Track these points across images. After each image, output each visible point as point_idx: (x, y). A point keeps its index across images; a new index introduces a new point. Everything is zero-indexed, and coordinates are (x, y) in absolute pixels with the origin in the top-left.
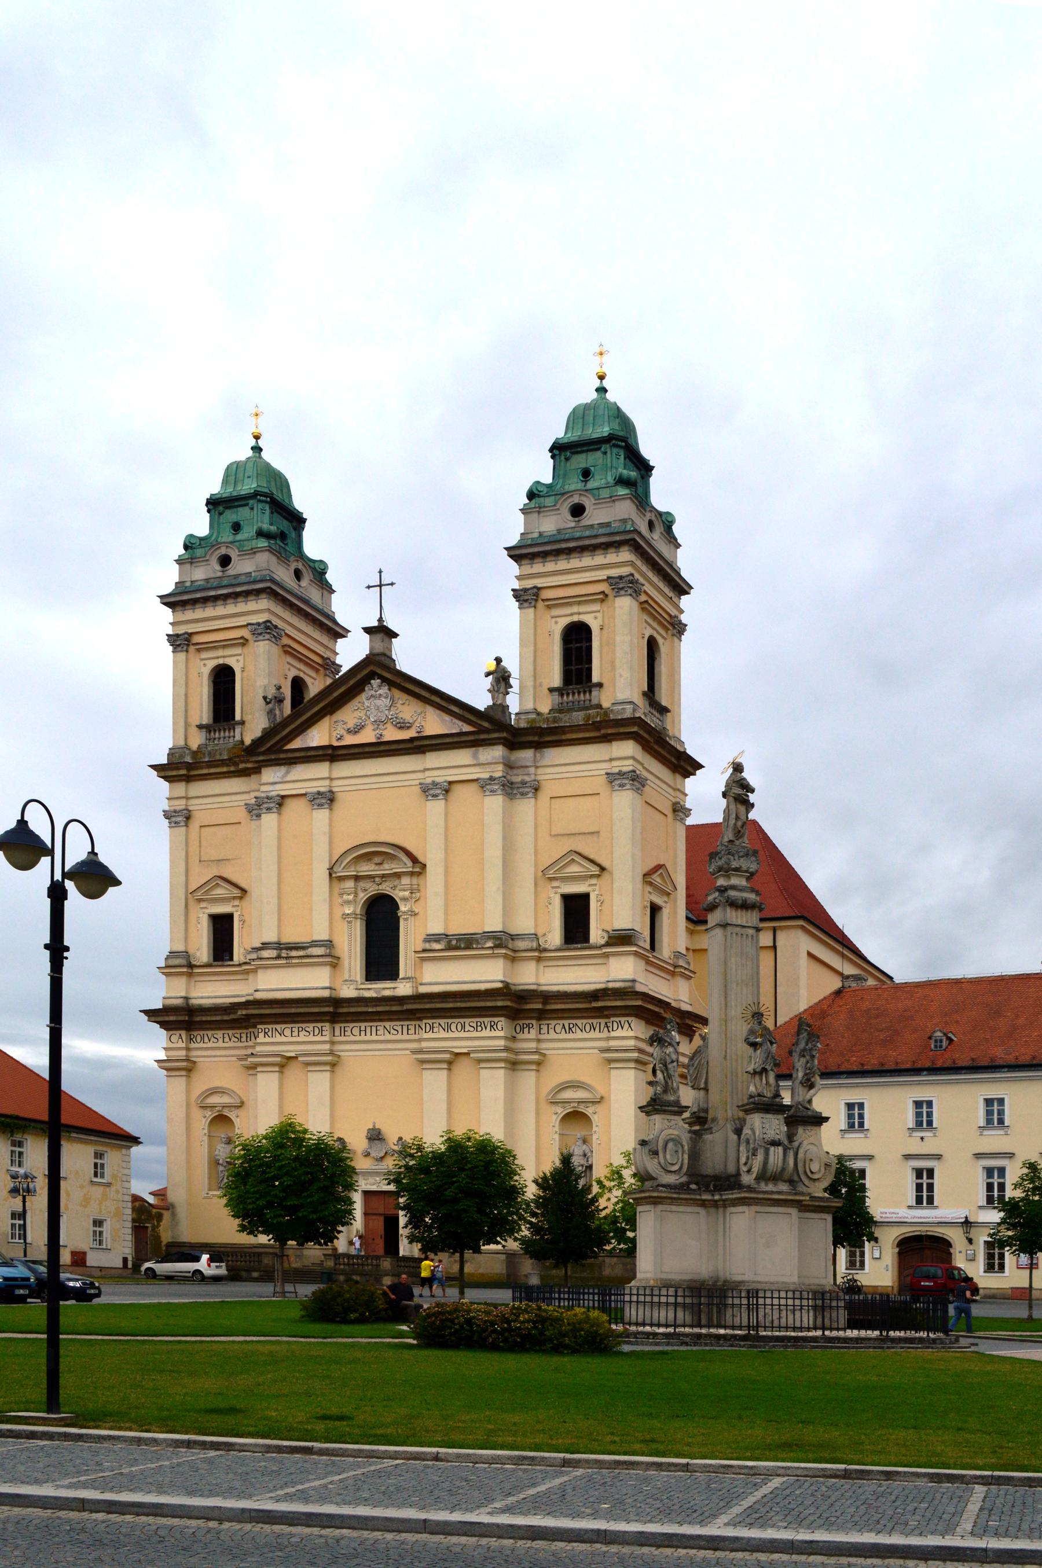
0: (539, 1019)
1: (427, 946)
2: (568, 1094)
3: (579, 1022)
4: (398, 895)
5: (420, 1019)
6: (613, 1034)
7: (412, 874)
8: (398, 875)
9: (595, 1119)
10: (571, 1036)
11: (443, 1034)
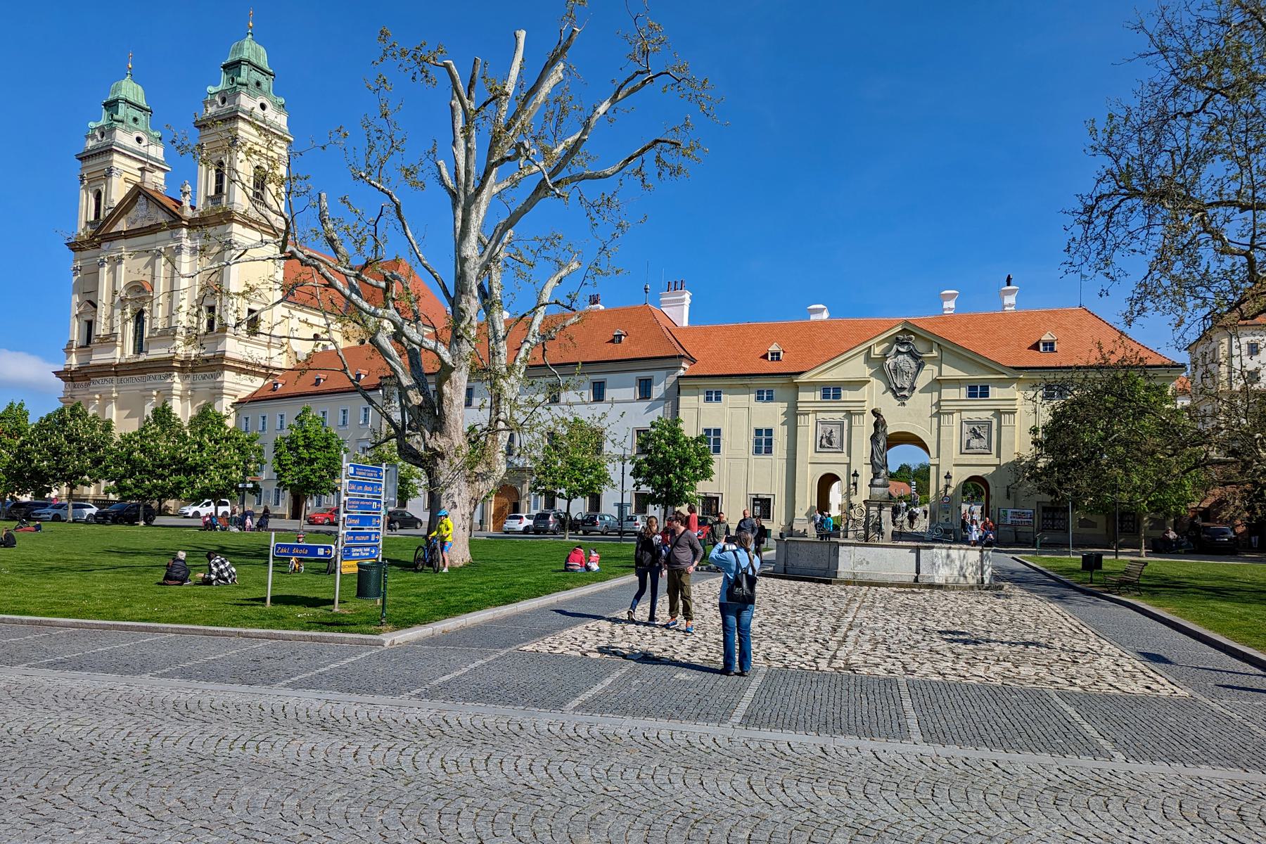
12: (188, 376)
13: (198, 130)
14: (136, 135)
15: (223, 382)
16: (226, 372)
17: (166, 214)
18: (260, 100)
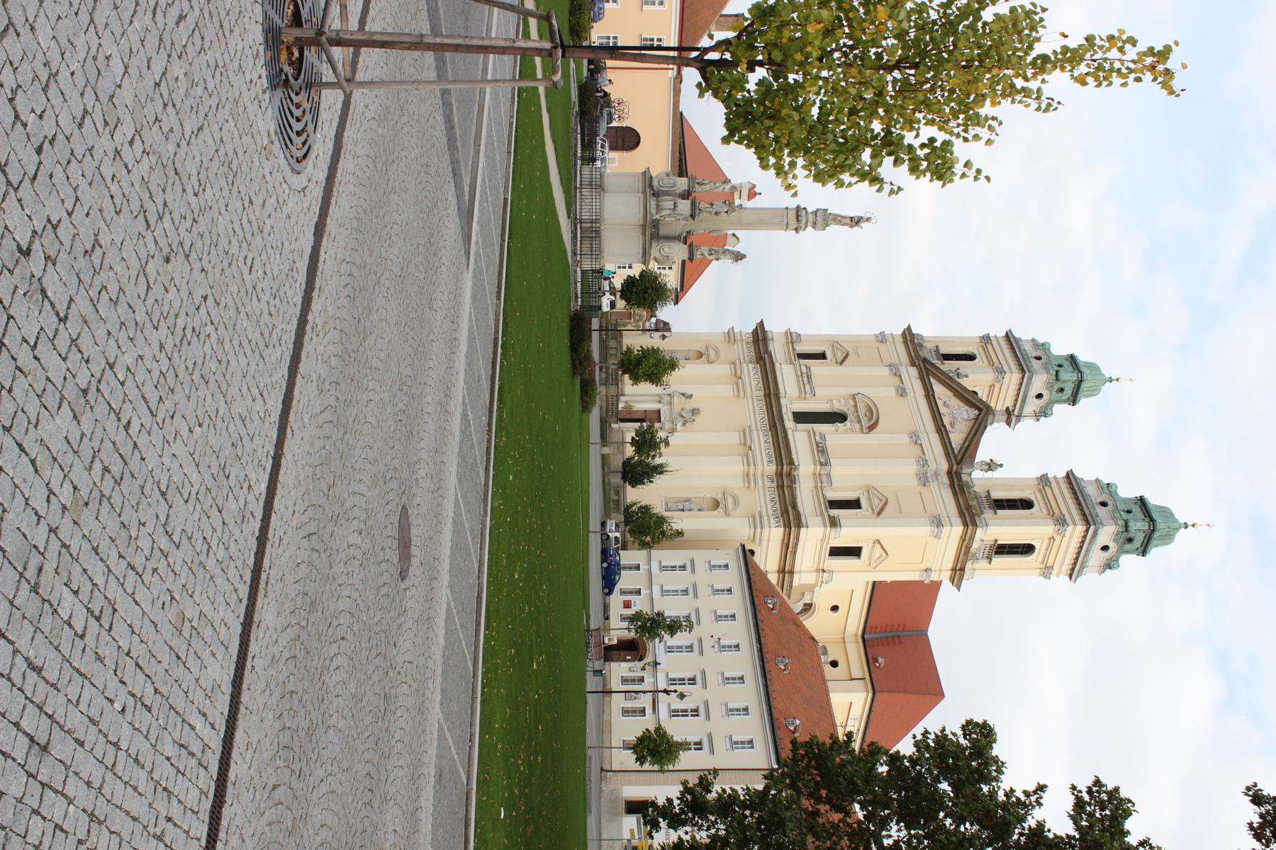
0: (778, 487)
1: (817, 434)
2: (730, 501)
3: (778, 505)
4: (847, 423)
5: (771, 430)
6: (772, 519)
7: (862, 429)
8: (860, 422)
9: (716, 512)
10: (768, 502)
11: (762, 440)
12: (772, 481)
13: (1064, 474)
14: (1045, 393)
15: (770, 527)
16: (781, 530)
17: (961, 442)
18: (1113, 547)
